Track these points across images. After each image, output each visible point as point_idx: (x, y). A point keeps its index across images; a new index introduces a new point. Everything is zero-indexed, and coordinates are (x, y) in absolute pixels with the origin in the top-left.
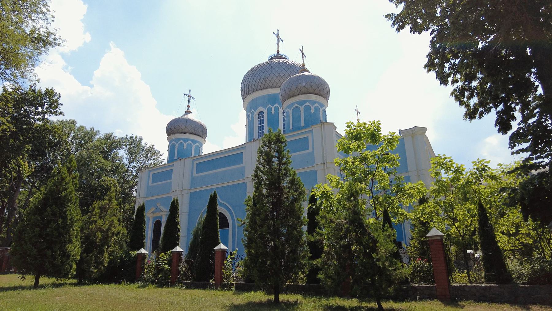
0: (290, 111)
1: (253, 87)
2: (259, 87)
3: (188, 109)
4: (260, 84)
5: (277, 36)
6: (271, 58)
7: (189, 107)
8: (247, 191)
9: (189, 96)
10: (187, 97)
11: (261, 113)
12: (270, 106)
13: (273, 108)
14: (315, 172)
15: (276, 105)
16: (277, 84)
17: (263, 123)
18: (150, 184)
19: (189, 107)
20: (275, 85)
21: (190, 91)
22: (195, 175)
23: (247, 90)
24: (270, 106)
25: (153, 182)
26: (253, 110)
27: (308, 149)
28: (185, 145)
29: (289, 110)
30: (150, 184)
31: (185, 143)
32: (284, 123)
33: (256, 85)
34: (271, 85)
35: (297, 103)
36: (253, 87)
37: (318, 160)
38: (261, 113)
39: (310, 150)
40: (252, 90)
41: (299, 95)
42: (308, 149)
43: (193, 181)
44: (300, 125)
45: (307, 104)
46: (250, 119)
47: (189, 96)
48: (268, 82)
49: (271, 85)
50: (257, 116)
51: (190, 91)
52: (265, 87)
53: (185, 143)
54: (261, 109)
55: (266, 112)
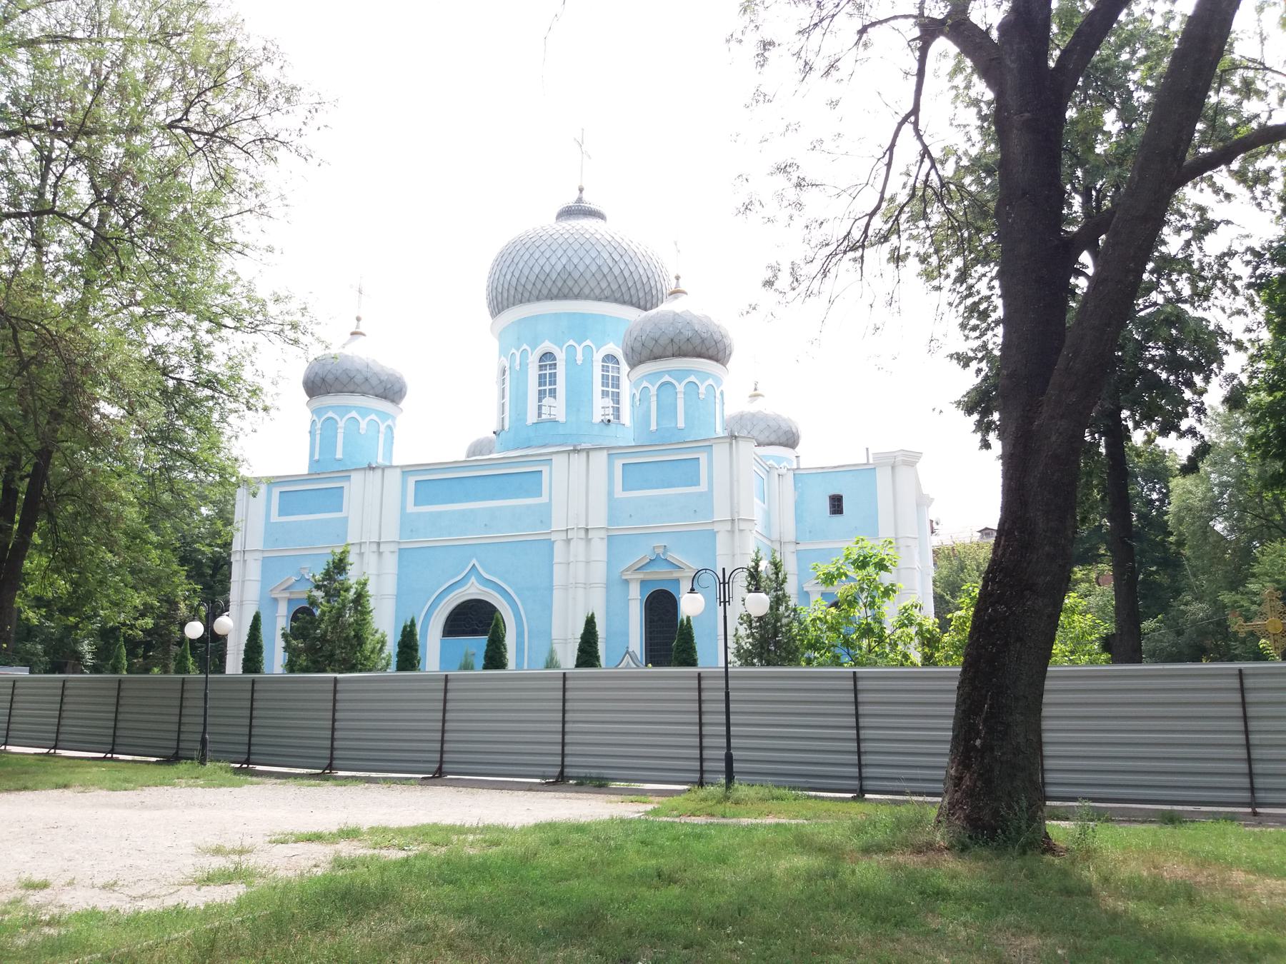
0: (653, 390)
1: (529, 287)
2: (545, 292)
3: (358, 327)
4: (549, 283)
6: (568, 213)
8: (556, 560)
11: (547, 356)
12: (571, 342)
13: (579, 350)
14: (714, 534)
15: (588, 342)
16: (592, 290)
17: (553, 382)
18: (275, 518)
20: (587, 291)
22: (411, 508)
23: (512, 292)
24: (571, 342)
25: (282, 512)
26: (525, 346)
27: (697, 484)
28: (363, 424)
29: (650, 386)
30: (275, 518)
31: (363, 419)
32: (605, 389)
33: (539, 285)
34: (576, 290)
35: (669, 372)
36: (529, 287)
37: (721, 512)
38: (547, 356)
39: (703, 487)
40: (526, 295)
42: (697, 484)
43: (406, 522)
44: (673, 425)
45: (692, 378)
46: (518, 368)
48: (570, 283)
50: (537, 364)
53: (363, 419)
54: (547, 346)
55: (561, 356)
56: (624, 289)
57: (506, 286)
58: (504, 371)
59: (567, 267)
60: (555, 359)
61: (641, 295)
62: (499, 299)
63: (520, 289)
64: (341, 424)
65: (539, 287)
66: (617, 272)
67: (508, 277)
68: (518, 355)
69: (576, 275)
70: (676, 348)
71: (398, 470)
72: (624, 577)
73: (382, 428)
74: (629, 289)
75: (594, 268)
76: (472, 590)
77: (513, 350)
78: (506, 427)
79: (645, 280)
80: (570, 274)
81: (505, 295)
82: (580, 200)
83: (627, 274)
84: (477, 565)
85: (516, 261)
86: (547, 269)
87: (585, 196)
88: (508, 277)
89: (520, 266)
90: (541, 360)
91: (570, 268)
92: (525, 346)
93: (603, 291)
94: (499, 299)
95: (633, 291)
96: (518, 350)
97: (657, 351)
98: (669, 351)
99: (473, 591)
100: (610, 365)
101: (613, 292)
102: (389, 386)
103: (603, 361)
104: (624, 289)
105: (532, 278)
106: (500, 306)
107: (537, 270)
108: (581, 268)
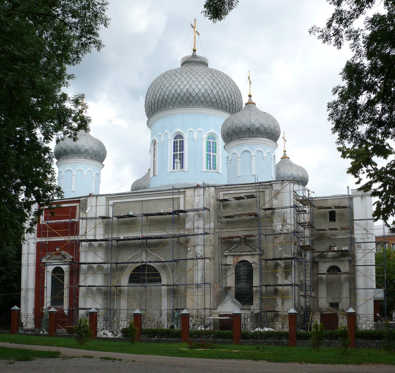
24: (191, 129)
55: (186, 137)
59: (189, 90)
60: (182, 138)
61: (227, 105)
62: (153, 107)
63: (164, 102)
64: (74, 173)
66: (215, 92)
67: (158, 96)
71: (104, 197)
75: (203, 91)
79: (229, 97)
81: (156, 105)
82: (194, 56)
83: (220, 94)
85: (162, 87)
86: (179, 91)
87: (197, 53)
88: (158, 96)
89: (164, 90)
90: (175, 139)
91: (190, 90)
92: (166, 131)
94: (153, 107)
96: (163, 133)
100: (211, 141)
102: (98, 153)
105: (171, 96)
106: (153, 111)
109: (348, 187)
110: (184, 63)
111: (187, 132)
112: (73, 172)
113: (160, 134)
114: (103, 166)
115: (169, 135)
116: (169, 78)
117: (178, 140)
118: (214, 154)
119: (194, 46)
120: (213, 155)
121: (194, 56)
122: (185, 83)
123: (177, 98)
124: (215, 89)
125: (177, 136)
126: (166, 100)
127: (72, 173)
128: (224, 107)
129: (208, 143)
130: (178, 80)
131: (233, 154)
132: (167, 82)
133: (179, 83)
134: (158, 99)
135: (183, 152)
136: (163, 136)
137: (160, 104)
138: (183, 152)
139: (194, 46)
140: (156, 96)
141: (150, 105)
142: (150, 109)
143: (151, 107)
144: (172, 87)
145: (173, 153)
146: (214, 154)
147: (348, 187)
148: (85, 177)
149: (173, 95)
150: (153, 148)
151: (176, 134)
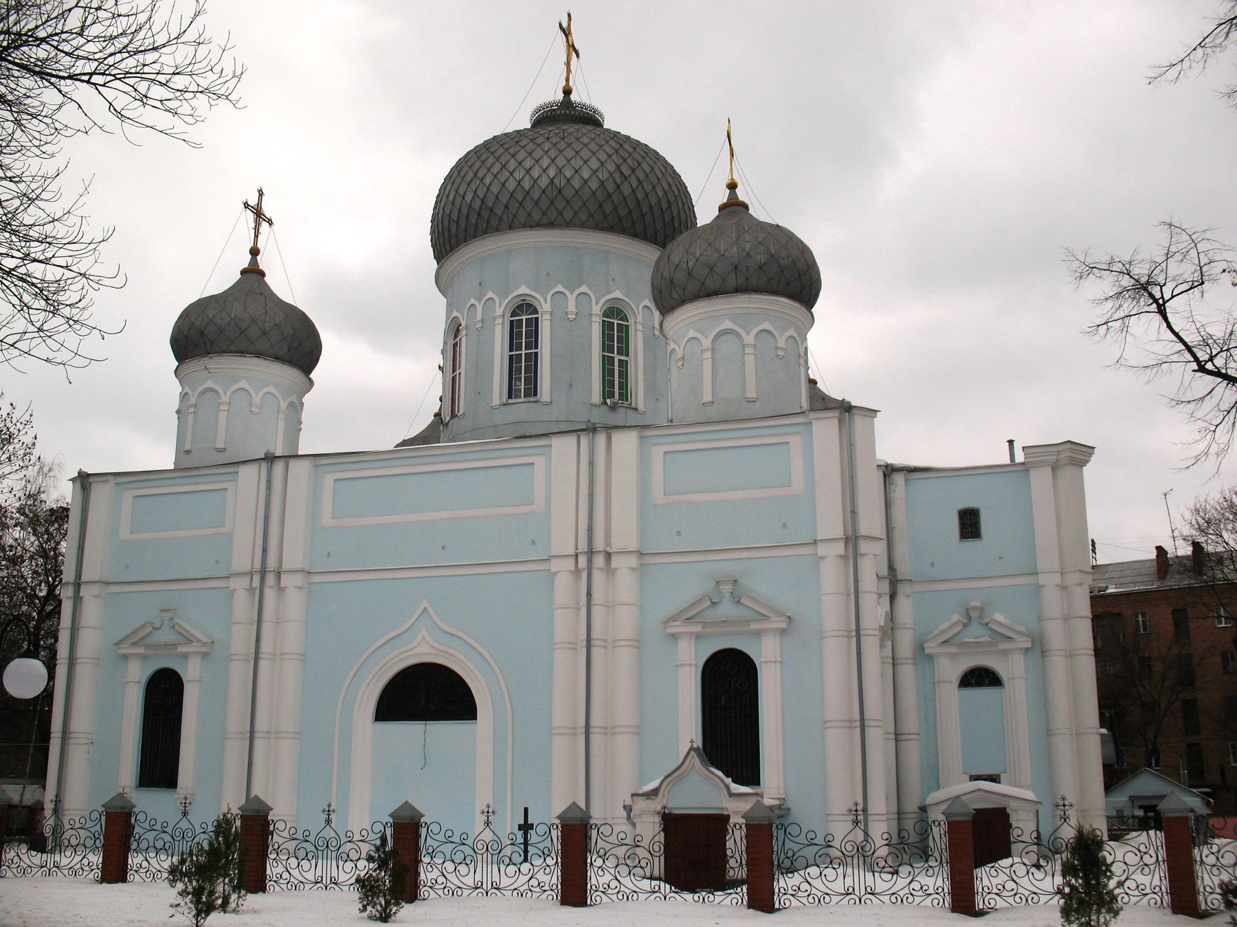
0: (707, 342)
2: (522, 217)
3: (254, 261)
4: (528, 205)
5: (567, 36)
7: (255, 252)
9: (258, 213)
10: (251, 216)
11: (525, 306)
13: (572, 299)
15: (584, 289)
18: (125, 534)
19: (255, 252)
21: (261, 193)
24: (560, 288)
30: (125, 534)
34: (568, 215)
40: (494, 222)
41: (738, 290)
47: (258, 213)
49: (568, 215)
51: (261, 193)
52: (545, 221)
55: (545, 306)
56: (636, 215)
57: (465, 212)
58: (458, 331)
59: (556, 182)
61: (659, 226)
62: (453, 230)
63: (485, 214)
64: (225, 398)
65: (514, 211)
67: (469, 198)
68: (479, 307)
69: (569, 193)
70: (741, 278)
72: (670, 630)
73: (284, 405)
74: (643, 216)
75: (594, 185)
76: (424, 649)
77: (473, 301)
78: (462, 408)
79: (665, 206)
80: (560, 191)
81: (463, 224)
82: (567, 103)
83: (640, 195)
84: (430, 610)
85: (480, 174)
86: (527, 184)
88: (469, 198)
90: (513, 314)
92: (490, 295)
93: (606, 217)
94: (453, 230)
95: (648, 219)
96: (479, 301)
97: (710, 284)
98: (731, 282)
99: (423, 651)
100: (616, 322)
101: (620, 219)
103: (606, 314)
104: (636, 215)
105: (504, 198)
106: (454, 241)
107: (511, 185)
108: (576, 183)
109: (1011, 442)
110: (539, 121)
111: (550, 295)
112: (222, 395)
113: (473, 301)
114: (311, 382)
115: (498, 304)
116: (501, 150)
117: (524, 318)
118: (623, 358)
119: (567, 80)
120: (619, 360)
121: (567, 103)
122: (545, 162)
123: (521, 204)
124: (626, 183)
125: (520, 307)
126: (492, 210)
127: (220, 397)
128: (650, 232)
129: (607, 327)
130: (526, 154)
131: (688, 341)
132: (495, 160)
133: (528, 163)
134: (470, 206)
135: (536, 351)
136: (479, 307)
137: (473, 220)
138: (536, 351)
139: (567, 80)
140: (463, 198)
141: (446, 224)
142: (447, 235)
143: (449, 230)
144: (508, 174)
145: (507, 353)
146: (623, 358)
147: (1011, 442)
148: (257, 410)
149: (512, 195)
150: (451, 342)
151: (518, 302)
